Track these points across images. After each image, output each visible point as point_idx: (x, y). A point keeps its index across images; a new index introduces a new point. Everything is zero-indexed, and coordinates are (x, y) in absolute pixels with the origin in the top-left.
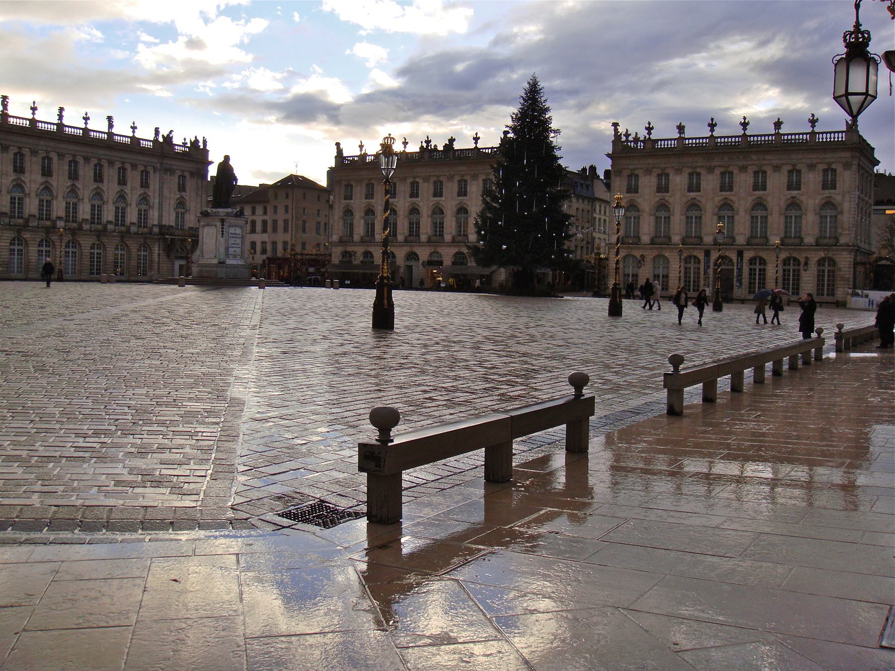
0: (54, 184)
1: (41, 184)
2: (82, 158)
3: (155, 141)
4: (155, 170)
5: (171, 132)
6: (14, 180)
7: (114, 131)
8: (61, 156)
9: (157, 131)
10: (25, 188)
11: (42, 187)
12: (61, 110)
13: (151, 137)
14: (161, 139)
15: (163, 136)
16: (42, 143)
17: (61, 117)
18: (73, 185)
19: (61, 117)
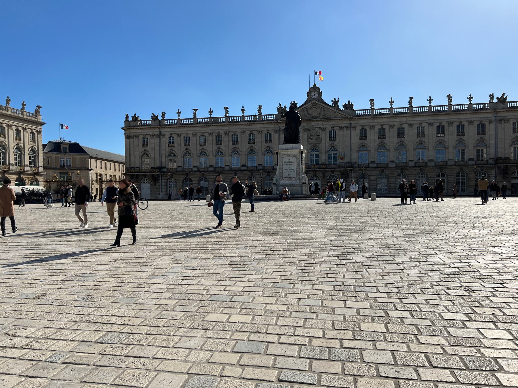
0: (407, 142)
1: (398, 143)
2: (427, 124)
3: (491, 103)
4: (490, 122)
5: (504, 94)
6: (379, 143)
7: (453, 103)
8: (411, 125)
9: (492, 96)
10: (387, 147)
11: (398, 145)
12: (411, 98)
13: (487, 100)
14: (495, 101)
15: (498, 98)
16: (397, 120)
17: (411, 103)
18: (421, 141)
19: (411, 103)
